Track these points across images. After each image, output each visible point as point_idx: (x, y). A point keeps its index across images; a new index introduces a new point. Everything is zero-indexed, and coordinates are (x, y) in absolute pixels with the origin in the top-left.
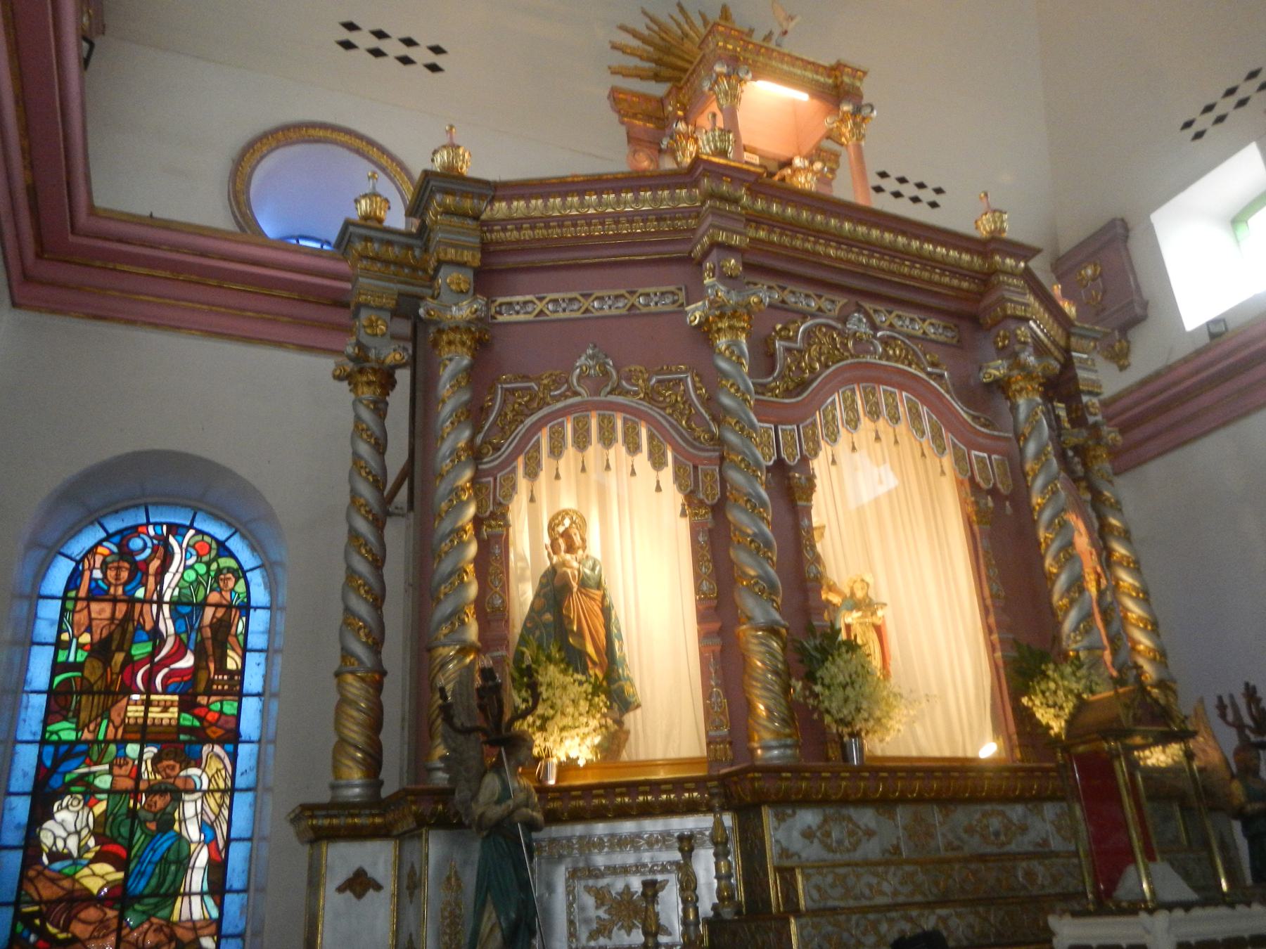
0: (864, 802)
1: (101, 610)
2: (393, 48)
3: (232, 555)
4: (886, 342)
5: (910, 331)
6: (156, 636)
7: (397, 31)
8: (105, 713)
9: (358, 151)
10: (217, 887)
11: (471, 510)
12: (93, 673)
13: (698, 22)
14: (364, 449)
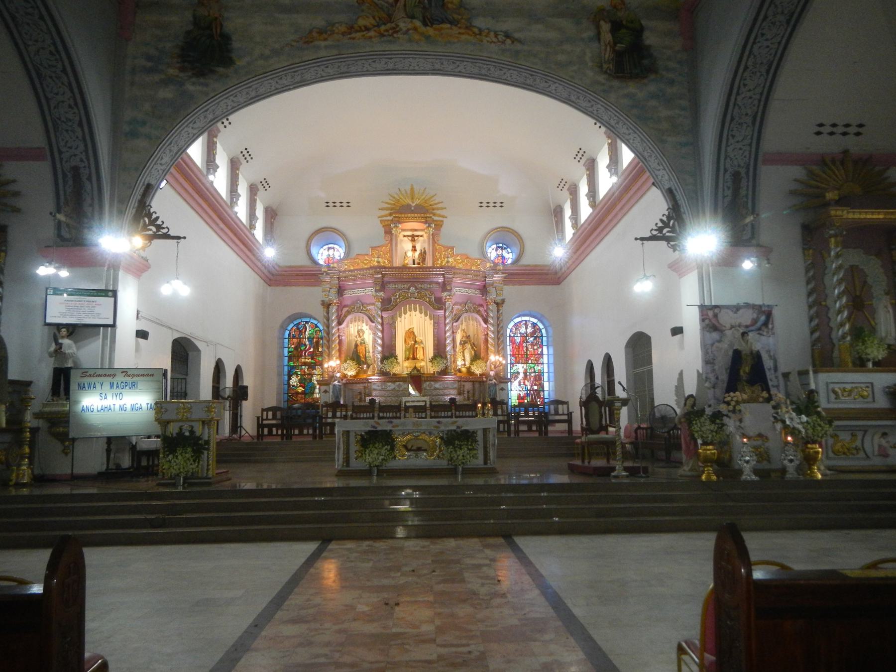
1: (295, 340)
2: (338, 204)
4: (418, 292)
5: (426, 287)
6: (305, 345)
7: (338, 201)
8: (298, 360)
9: (333, 232)
11: (337, 335)
12: (295, 352)
13: (403, 192)
14: (325, 320)
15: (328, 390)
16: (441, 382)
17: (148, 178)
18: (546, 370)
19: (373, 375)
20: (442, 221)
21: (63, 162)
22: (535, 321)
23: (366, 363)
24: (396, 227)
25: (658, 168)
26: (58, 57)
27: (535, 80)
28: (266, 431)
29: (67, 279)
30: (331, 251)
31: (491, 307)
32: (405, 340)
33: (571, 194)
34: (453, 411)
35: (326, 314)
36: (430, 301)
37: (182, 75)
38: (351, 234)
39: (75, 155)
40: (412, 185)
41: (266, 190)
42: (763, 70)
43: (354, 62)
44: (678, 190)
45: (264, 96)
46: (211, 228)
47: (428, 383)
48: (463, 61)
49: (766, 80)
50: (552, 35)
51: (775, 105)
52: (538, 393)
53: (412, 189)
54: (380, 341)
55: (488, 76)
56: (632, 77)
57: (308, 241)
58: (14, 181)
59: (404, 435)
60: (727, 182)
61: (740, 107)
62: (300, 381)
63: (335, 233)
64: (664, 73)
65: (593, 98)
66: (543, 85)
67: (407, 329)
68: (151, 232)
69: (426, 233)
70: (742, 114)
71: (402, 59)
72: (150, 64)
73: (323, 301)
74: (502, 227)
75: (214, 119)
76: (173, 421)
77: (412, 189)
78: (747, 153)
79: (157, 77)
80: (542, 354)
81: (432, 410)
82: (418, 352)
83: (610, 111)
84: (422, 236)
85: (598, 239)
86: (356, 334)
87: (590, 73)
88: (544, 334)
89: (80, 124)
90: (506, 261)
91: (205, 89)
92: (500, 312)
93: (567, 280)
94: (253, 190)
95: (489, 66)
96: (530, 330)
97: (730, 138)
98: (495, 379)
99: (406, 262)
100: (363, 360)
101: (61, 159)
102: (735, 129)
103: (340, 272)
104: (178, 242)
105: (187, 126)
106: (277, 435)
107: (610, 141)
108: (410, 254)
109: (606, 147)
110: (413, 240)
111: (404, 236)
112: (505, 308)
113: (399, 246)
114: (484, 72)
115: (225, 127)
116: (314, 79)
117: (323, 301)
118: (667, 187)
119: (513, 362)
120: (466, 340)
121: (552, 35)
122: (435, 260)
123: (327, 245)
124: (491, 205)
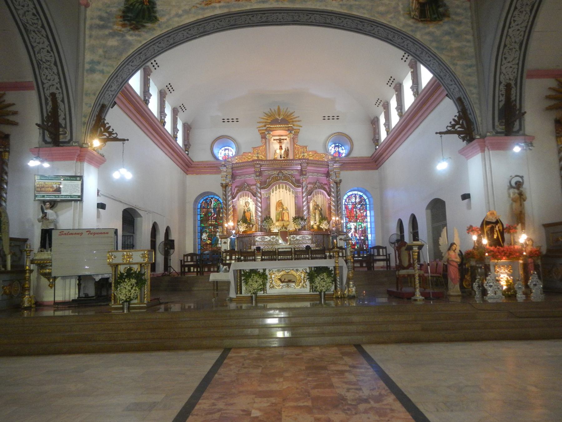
0: (265, 235)
1: (205, 210)
2: (230, 120)
3: (219, 201)
7: (230, 118)
8: (207, 223)
9: (228, 138)
11: (232, 205)
15: (226, 242)
16: (301, 236)
17: (103, 100)
18: (369, 226)
19: (256, 232)
20: (299, 129)
21: (45, 90)
22: (361, 194)
23: (249, 224)
24: (269, 133)
25: (451, 83)
26: (38, 17)
27: (363, 25)
28: (186, 269)
29: (48, 168)
30: (227, 151)
31: (332, 185)
32: (276, 208)
33: (384, 109)
34: (310, 254)
35: (224, 192)
36: (292, 182)
37: (123, 29)
38: (240, 140)
39: (53, 85)
40: (279, 106)
41: (184, 112)
42: (528, 9)
43: (239, 17)
44: (465, 98)
45: (179, 43)
46: (147, 135)
47: (292, 236)
48: (314, 14)
49: (530, 16)
51: (535, 35)
53: (279, 109)
54: (260, 209)
55: (331, 24)
56: (432, 20)
57: (212, 145)
58: (14, 104)
59: (279, 271)
60: (501, 91)
61: (510, 37)
62: (208, 236)
63: (230, 139)
64: (454, 17)
65: (405, 36)
66: (369, 28)
67: (277, 201)
68: (105, 137)
69: (288, 137)
70: (513, 42)
71: (272, 14)
72: (102, 23)
73: (222, 184)
74: (338, 133)
75: (146, 59)
76: (120, 264)
77: (279, 109)
78: (515, 70)
79: (107, 32)
80: (366, 216)
81: (295, 254)
82: (285, 216)
83: (417, 45)
84: (286, 139)
85: (404, 138)
86: (244, 205)
87: (402, 19)
88: (368, 203)
89: (55, 64)
90: (341, 155)
91: (139, 38)
92: (338, 189)
93: (382, 166)
94: (175, 112)
95: (332, 17)
96: (358, 200)
97: (503, 59)
98: (336, 233)
99: (276, 156)
100: (249, 221)
101: (43, 88)
102: (507, 53)
103: (233, 164)
104: (123, 143)
105: (127, 64)
106: (194, 272)
107: (412, 70)
108: (278, 151)
109: (410, 74)
110: (280, 142)
111: (274, 140)
112: (342, 186)
113: (271, 146)
114: (328, 21)
115: (155, 69)
116: (212, 30)
117: (222, 184)
118: (457, 97)
119: (347, 221)
120: (316, 207)
122: (295, 154)
123: (224, 147)
124: (331, 118)
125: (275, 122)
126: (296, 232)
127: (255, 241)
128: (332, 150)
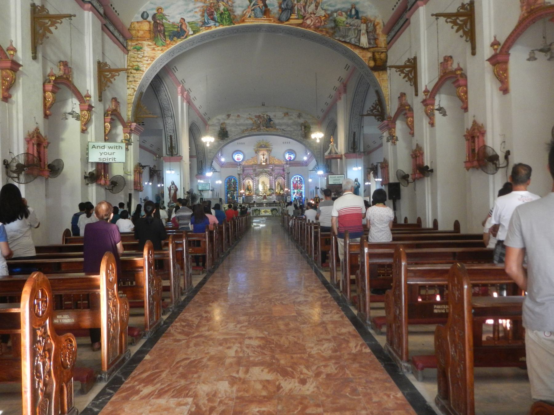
10: (237, 198)
50: (292, 129)
52: (301, 198)
53: (263, 140)
77: (263, 140)
80: (302, 187)
96: (299, 179)
108: (262, 159)
110: (263, 155)
112: (290, 175)
117: (238, 174)
120: (279, 184)
121: (292, 129)
122: (270, 161)
125: (261, 147)
126: (270, 195)
127: (253, 199)
128: (287, 156)
